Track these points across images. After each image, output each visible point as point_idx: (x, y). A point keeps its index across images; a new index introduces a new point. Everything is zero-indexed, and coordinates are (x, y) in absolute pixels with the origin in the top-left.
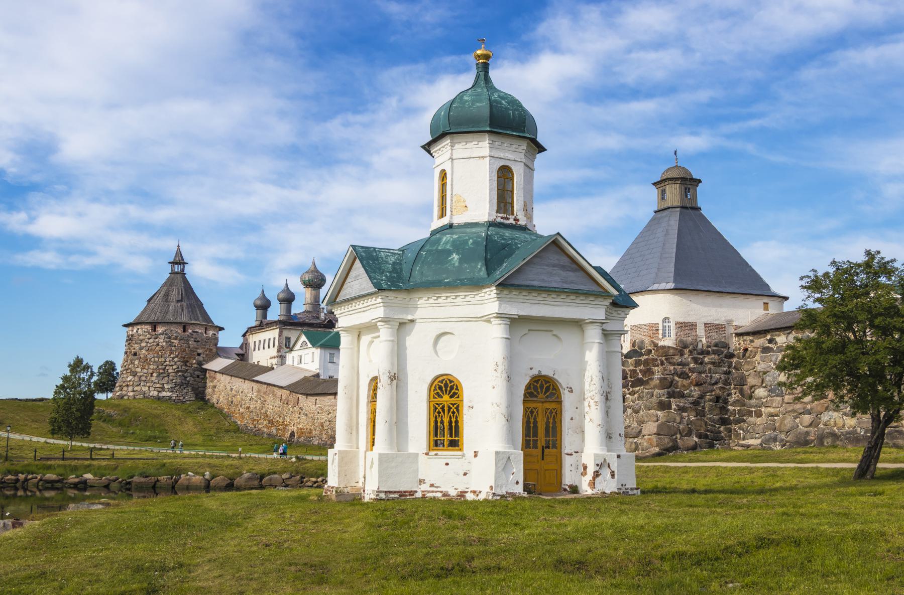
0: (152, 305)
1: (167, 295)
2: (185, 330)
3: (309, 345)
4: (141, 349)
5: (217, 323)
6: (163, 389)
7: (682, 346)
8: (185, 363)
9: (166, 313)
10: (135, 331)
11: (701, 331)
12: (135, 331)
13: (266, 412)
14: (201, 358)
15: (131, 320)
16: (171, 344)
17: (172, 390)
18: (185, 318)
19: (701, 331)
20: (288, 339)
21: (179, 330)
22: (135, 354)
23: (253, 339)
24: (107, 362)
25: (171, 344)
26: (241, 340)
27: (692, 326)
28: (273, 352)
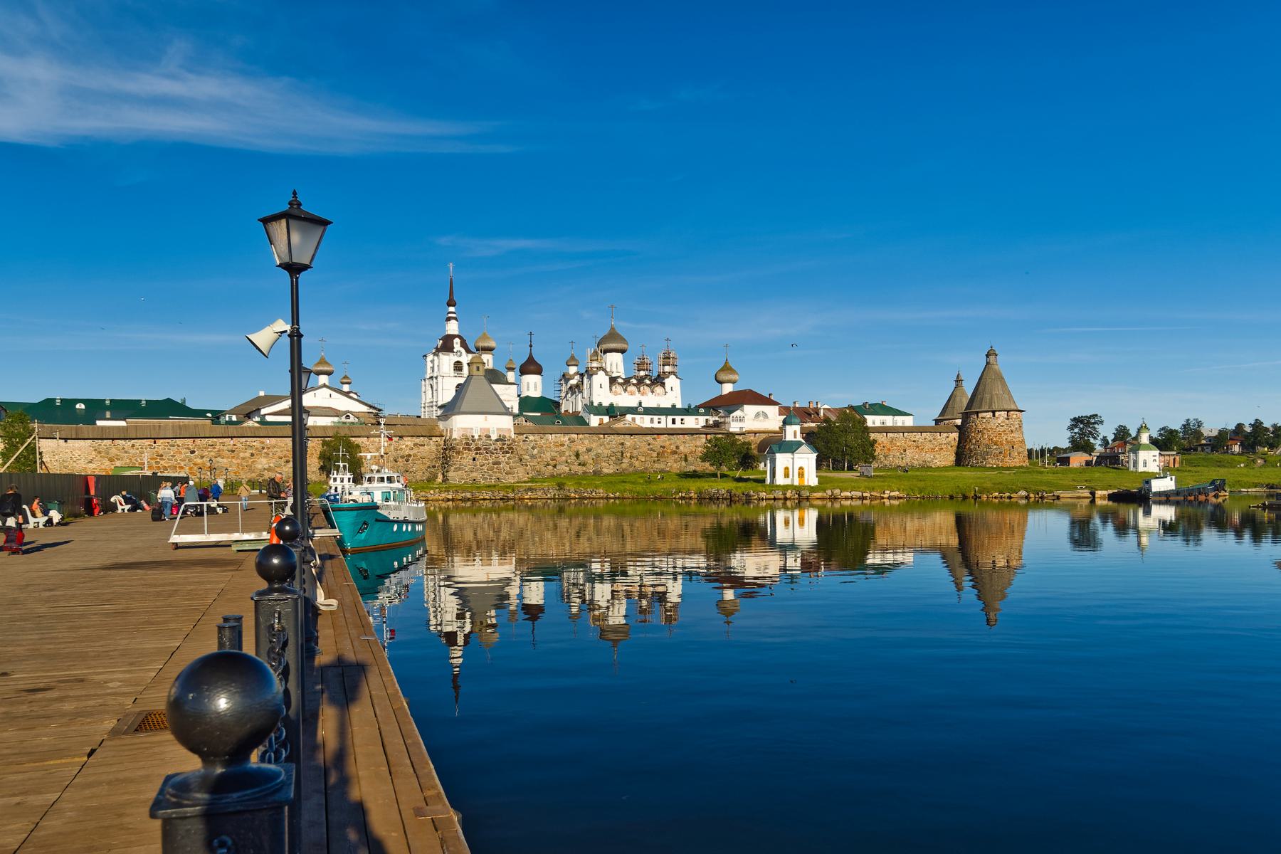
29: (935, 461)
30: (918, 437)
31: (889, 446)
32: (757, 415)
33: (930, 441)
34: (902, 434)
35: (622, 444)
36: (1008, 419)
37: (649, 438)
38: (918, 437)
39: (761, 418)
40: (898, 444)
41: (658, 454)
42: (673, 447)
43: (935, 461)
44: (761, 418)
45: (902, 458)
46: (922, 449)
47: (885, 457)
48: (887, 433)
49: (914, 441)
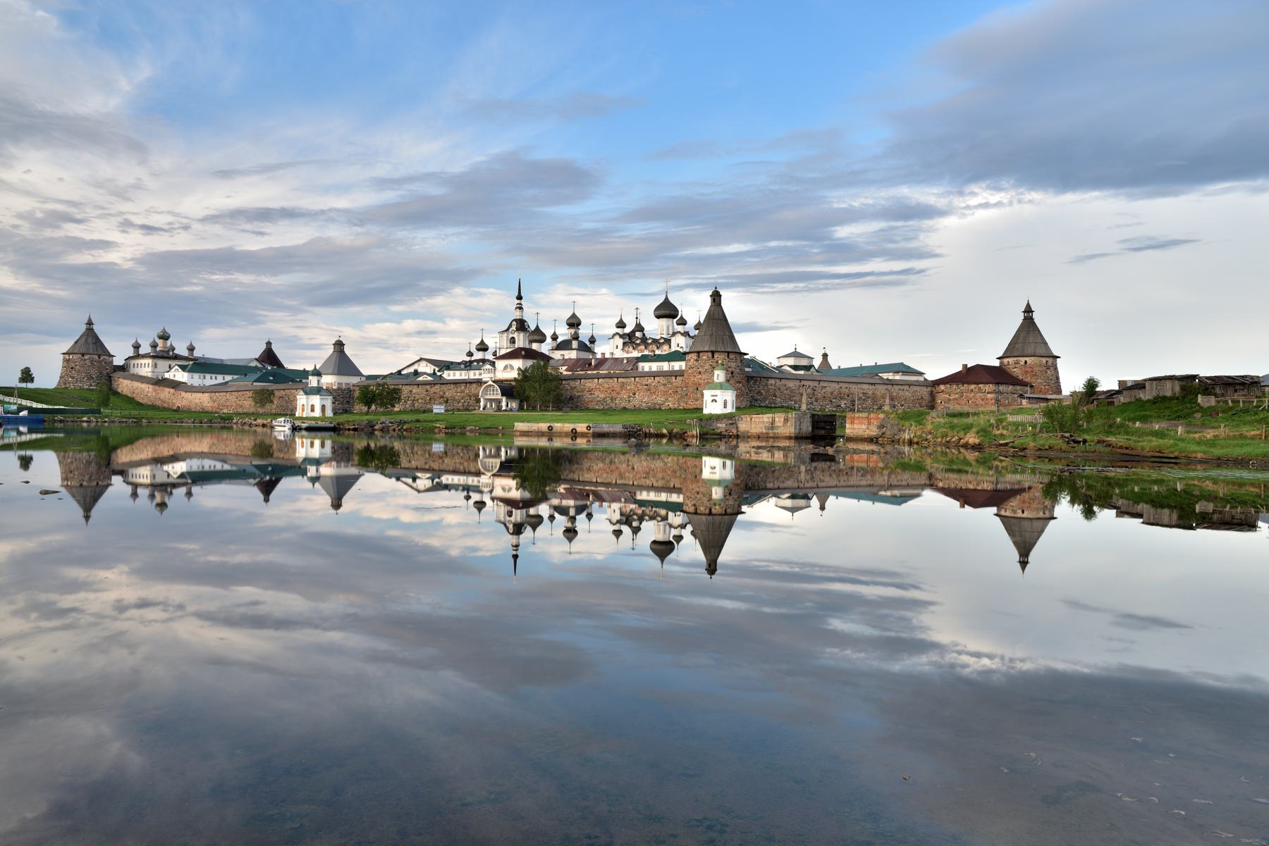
0: (79, 344)
1: (86, 340)
2: (99, 358)
3: (180, 370)
4: (76, 366)
5: (112, 354)
6: (91, 385)
7: (339, 389)
8: (101, 373)
9: (89, 349)
10: (71, 357)
11: (344, 385)
12: (71, 357)
13: (159, 398)
14: (107, 371)
15: (65, 352)
16: (93, 364)
17: (96, 386)
18: (100, 352)
19: (344, 385)
20: (156, 364)
21: (97, 357)
22: (72, 368)
23: (132, 362)
24: (27, 368)
25: (93, 364)
26: (124, 362)
27: (342, 384)
28: (150, 369)
29: (667, 404)
30: (650, 381)
31: (618, 390)
32: (506, 368)
33: (665, 385)
34: (633, 379)
35: (411, 391)
36: (697, 360)
37: (428, 387)
38: (650, 381)
39: (509, 369)
40: (628, 388)
41: (430, 399)
42: (441, 393)
43: (667, 404)
44: (509, 369)
45: (629, 401)
46: (654, 393)
47: (612, 399)
48: (598, 379)
49: (647, 385)
